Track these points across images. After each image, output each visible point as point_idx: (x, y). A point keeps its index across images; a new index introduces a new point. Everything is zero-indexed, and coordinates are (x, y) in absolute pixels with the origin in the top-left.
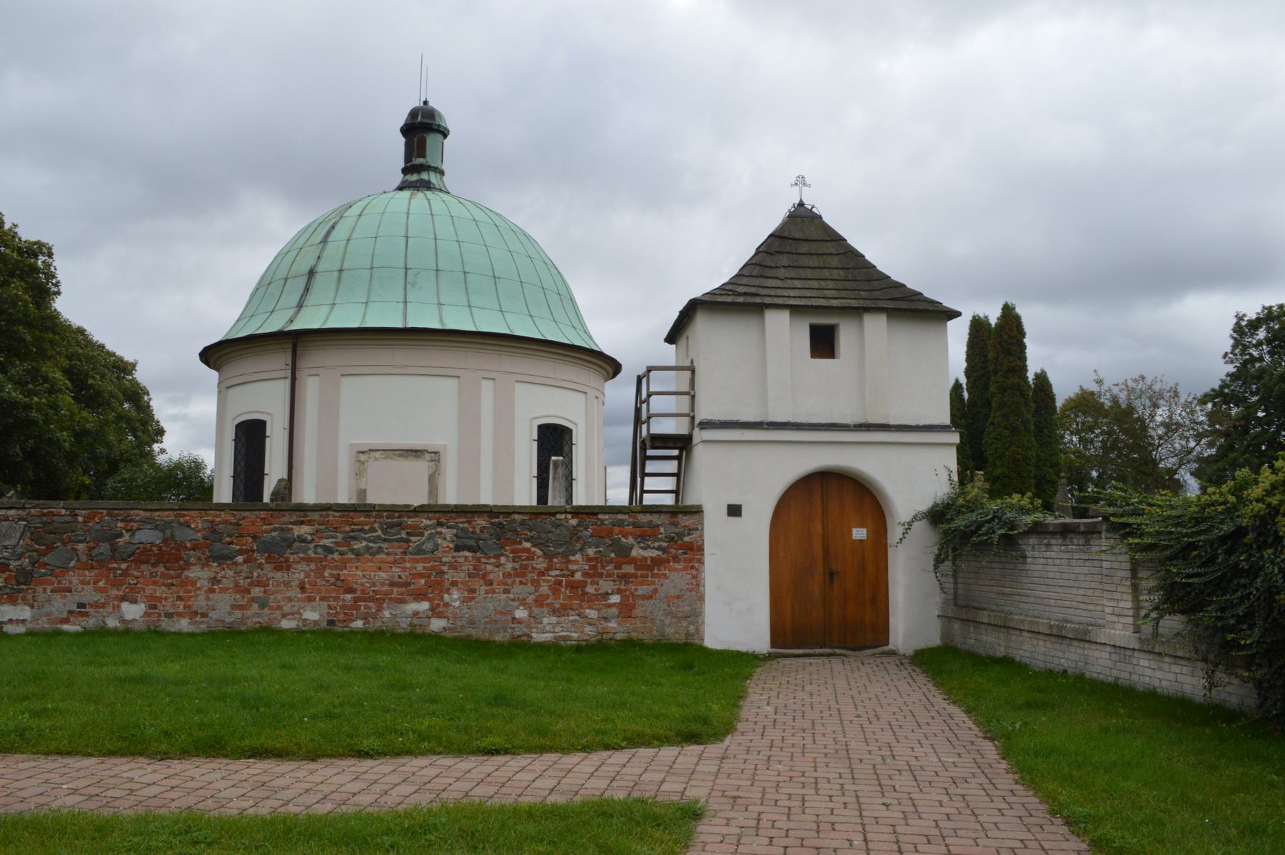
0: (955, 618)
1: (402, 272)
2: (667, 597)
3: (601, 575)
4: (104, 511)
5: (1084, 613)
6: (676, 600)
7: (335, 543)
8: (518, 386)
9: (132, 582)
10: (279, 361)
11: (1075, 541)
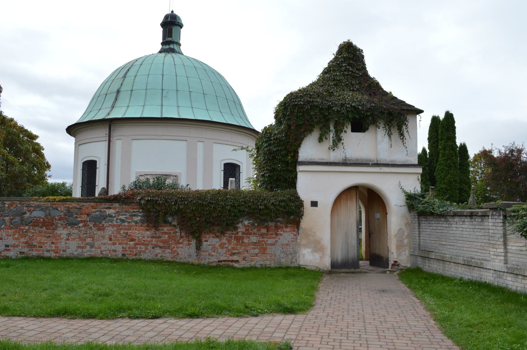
0: (419, 256)
1: (161, 91)
2: (282, 245)
3: (251, 234)
4: (18, 202)
5: (480, 254)
6: (286, 246)
7: (126, 217)
8: (214, 145)
9: (30, 235)
10: (103, 133)
11: (477, 220)
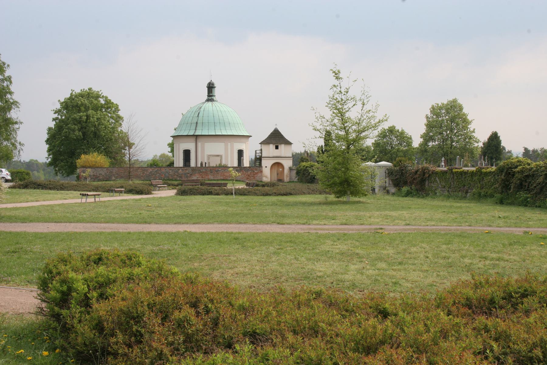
10: (194, 139)
